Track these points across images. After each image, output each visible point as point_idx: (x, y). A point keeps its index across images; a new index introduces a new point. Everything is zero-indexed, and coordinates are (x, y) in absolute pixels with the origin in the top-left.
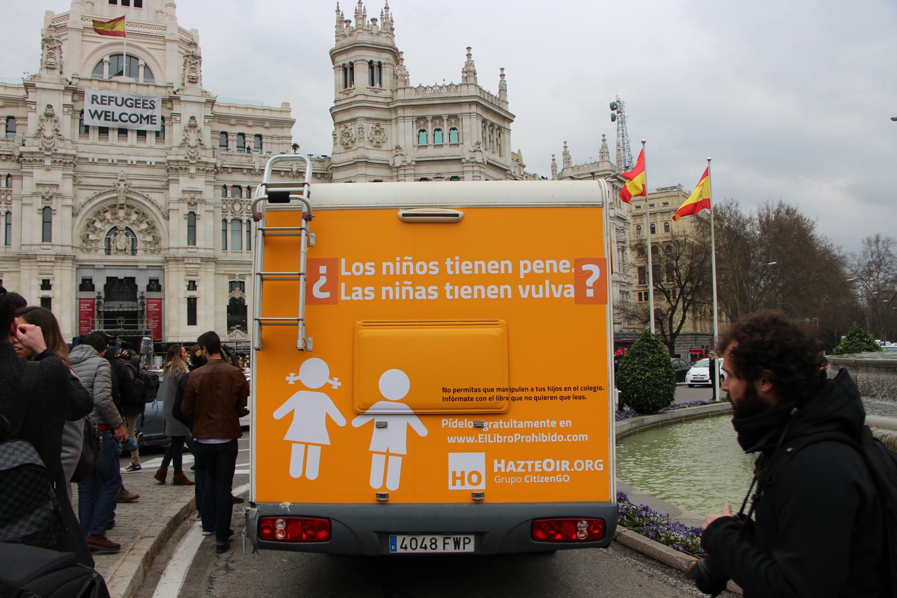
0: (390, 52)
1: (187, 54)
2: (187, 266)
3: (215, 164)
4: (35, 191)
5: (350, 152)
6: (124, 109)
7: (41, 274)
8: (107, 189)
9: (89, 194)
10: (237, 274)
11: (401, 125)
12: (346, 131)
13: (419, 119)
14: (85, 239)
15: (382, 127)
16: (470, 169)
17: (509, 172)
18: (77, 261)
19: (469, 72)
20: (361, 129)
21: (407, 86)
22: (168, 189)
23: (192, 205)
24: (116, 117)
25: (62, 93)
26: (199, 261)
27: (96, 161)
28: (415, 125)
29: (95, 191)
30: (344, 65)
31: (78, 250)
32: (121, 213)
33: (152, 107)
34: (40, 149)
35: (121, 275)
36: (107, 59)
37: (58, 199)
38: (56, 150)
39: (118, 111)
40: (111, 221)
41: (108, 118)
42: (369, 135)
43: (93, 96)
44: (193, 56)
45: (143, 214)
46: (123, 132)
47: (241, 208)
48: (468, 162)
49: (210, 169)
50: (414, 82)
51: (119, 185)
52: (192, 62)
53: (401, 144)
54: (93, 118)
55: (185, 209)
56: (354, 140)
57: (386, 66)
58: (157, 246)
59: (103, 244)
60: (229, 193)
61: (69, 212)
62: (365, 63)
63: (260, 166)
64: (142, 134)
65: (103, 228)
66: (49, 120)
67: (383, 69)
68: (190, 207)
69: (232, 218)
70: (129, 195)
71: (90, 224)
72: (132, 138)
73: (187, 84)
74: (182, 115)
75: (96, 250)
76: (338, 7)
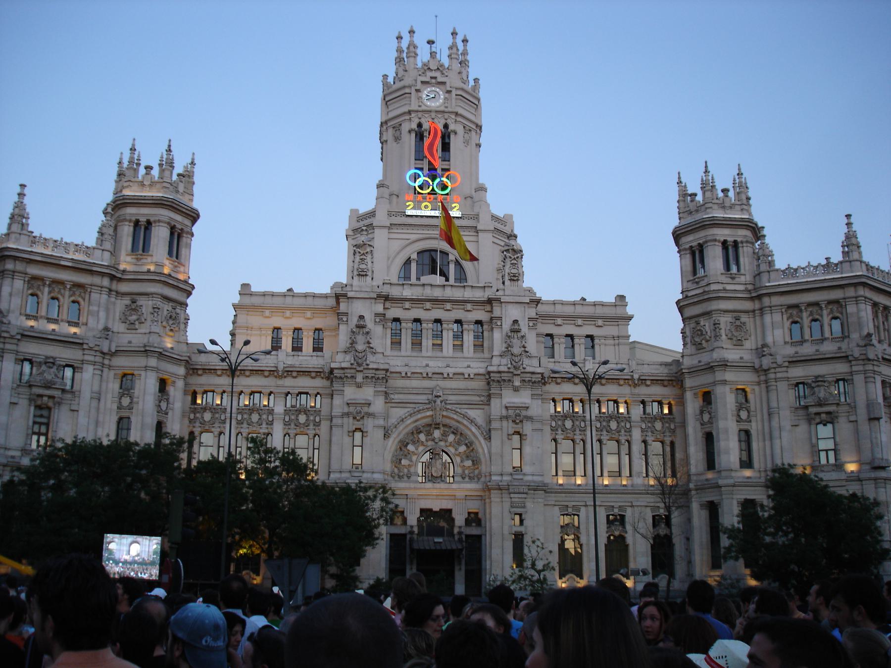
0: (747, 227)
1: (507, 248)
2: (512, 495)
3: (542, 374)
4: (346, 410)
5: (705, 354)
10: (571, 504)
11: (768, 318)
12: (699, 328)
13: (790, 307)
16: (861, 368)
19: (851, 243)
20: (716, 324)
21: (772, 269)
22: (489, 405)
23: (517, 424)
25: (373, 301)
26: (526, 491)
28: (785, 317)
29: (409, 409)
30: (691, 247)
31: (390, 478)
32: (437, 434)
34: (352, 364)
35: (436, 506)
36: (414, 256)
37: (370, 419)
38: (367, 365)
40: (425, 443)
42: (727, 331)
44: (513, 250)
45: (461, 433)
47: (573, 425)
48: (856, 359)
50: (780, 263)
51: (435, 402)
52: (513, 257)
53: (769, 340)
56: (708, 338)
57: (744, 245)
58: (476, 472)
61: (381, 433)
62: (717, 243)
66: (362, 333)
67: (740, 250)
68: (516, 426)
70: (445, 413)
73: (507, 283)
74: (503, 319)
75: (409, 477)
76: (679, 178)
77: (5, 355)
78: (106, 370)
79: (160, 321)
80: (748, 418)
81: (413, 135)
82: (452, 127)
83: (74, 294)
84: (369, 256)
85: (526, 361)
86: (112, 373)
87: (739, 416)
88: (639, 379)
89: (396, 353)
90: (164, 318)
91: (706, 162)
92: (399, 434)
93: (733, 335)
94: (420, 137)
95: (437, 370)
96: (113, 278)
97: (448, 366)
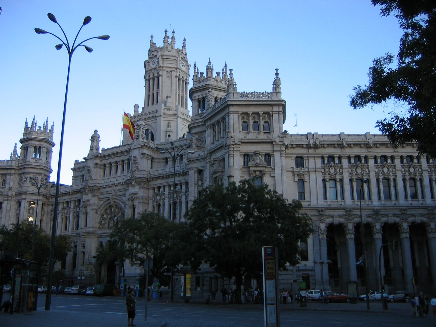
7: (82, 241)
9: (102, 202)
13: (213, 125)
14: (100, 223)
15: (203, 136)
16: (227, 150)
17: (274, 143)
27: (105, 186)
32: (113, 209)
47: (160, 198)
49: (141, 181)
55: (130, 203)
63: (166, 174)
65: (107, 218)
68: (133, 202)
70: (114, 200)
71: (102, 216)
78: (12, 202)
80: (202, 185)
83: (3, 178)
84: (95, 141)
87: (198, 184)
88: (183, 172)
89: (104, 178)
91: (195, 62)
92: (101, 210)
93: (197, 144)
95: (113, 183)
96: (15, 169)
97: (117, 180)
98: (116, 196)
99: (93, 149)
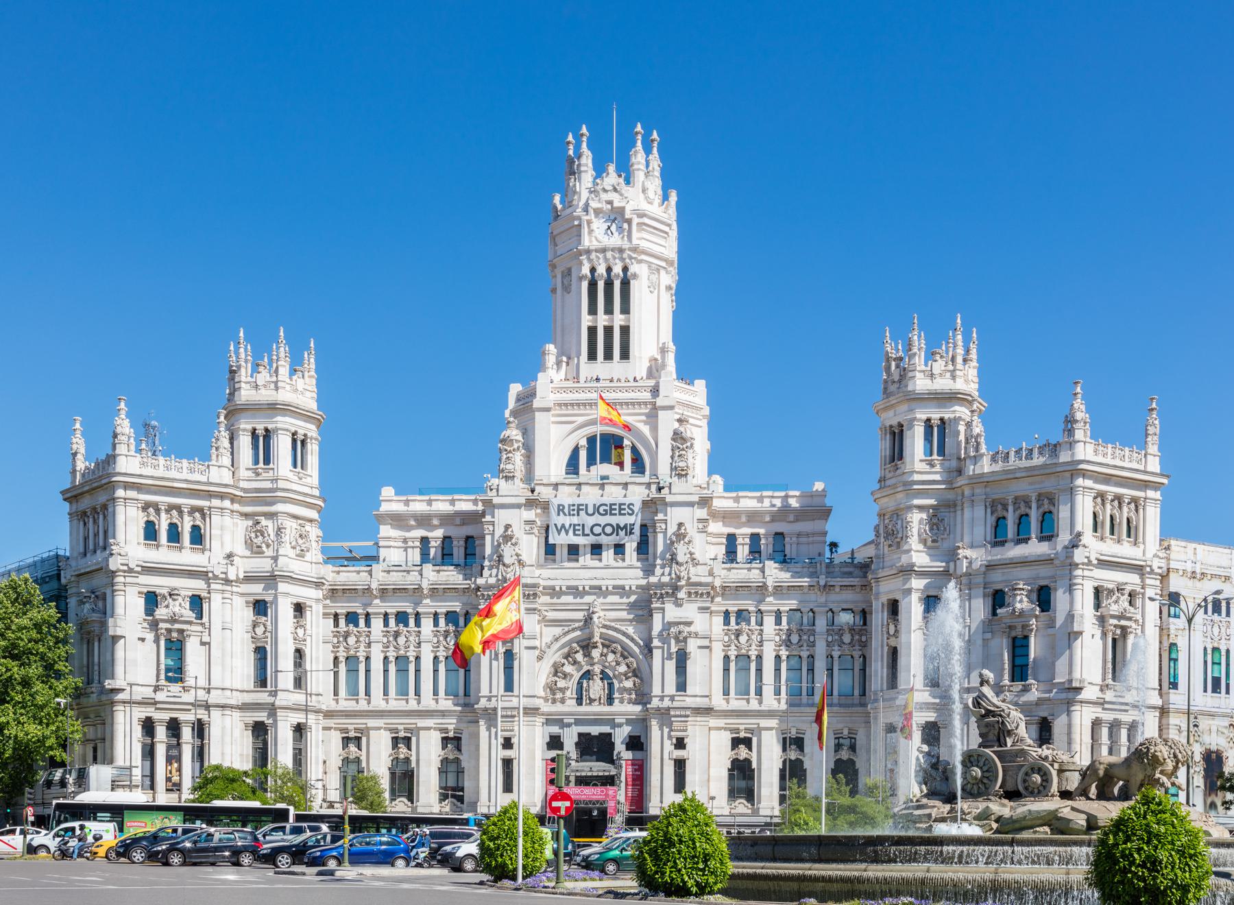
6: (597, 519)
8: (577, 625)
14: (552, 688)
18: (543, 715)
24: (587, 531)
32: (596, 653)
33: (630, 512)
39: (590, 521)
40: (583, 663)
41: (577, 532)
43: (559, 506)
46: (596, 549)
51: (591, 619)
54: (559, 534)
59: (574, 692)
60: (733, 620)
64: (619, 549)
69: (736, 653)
71: (557, 670)
72: (608, 555)
75: (563, 701)
77: (127, 589)
79: (288, 544)
81: (585, 285)
82: (633, 269)
85: (693, 570)
86: (244, 599)
90: (292, 539)
94: (593, 285)
98: (610, 621)
99: (514, 477)
